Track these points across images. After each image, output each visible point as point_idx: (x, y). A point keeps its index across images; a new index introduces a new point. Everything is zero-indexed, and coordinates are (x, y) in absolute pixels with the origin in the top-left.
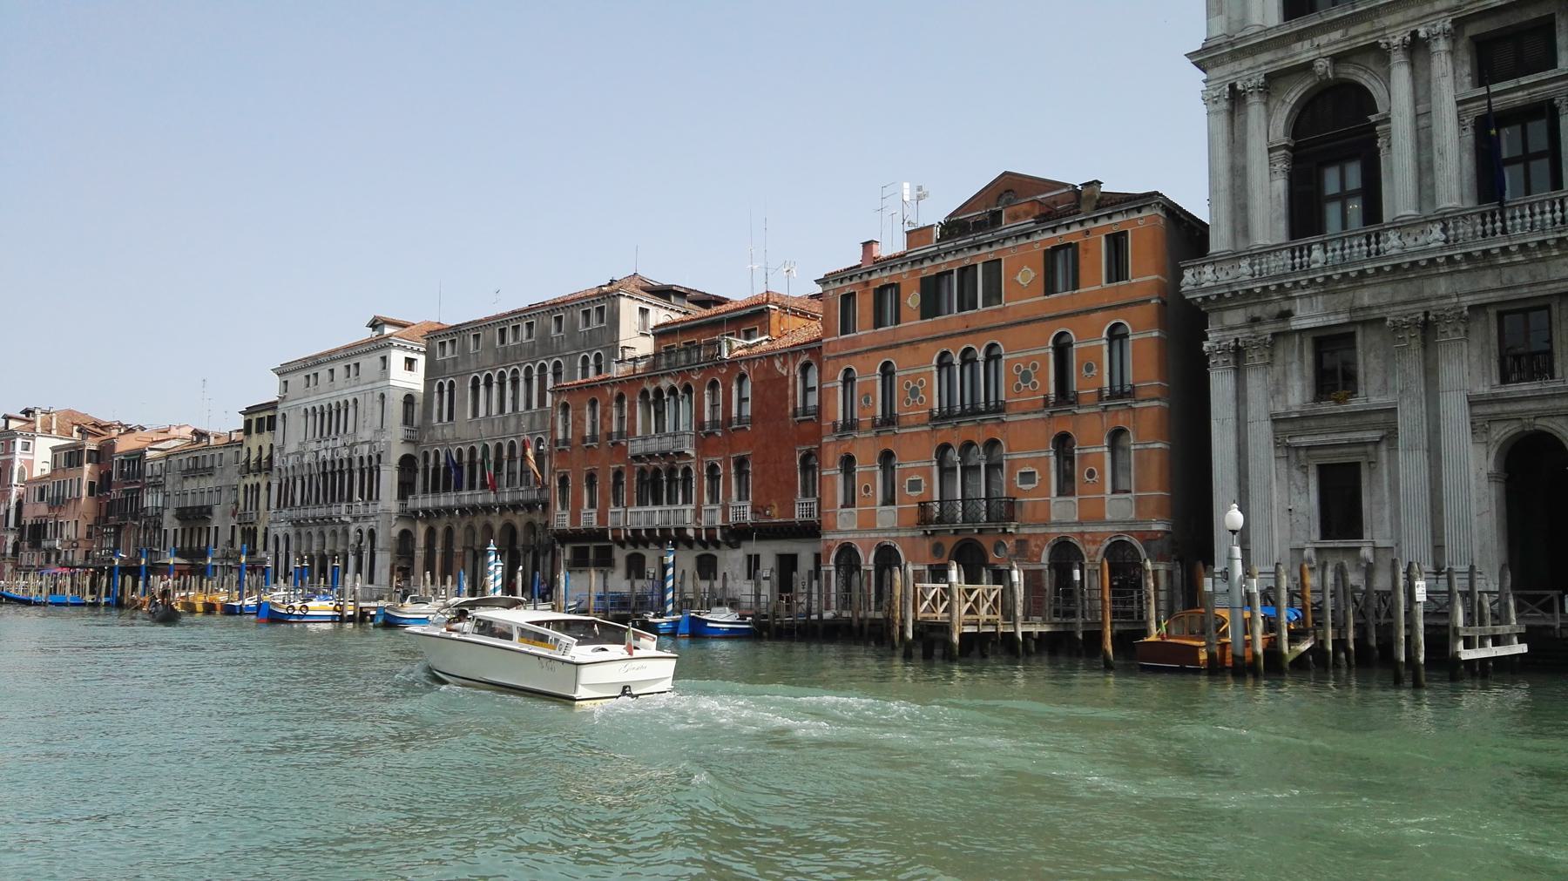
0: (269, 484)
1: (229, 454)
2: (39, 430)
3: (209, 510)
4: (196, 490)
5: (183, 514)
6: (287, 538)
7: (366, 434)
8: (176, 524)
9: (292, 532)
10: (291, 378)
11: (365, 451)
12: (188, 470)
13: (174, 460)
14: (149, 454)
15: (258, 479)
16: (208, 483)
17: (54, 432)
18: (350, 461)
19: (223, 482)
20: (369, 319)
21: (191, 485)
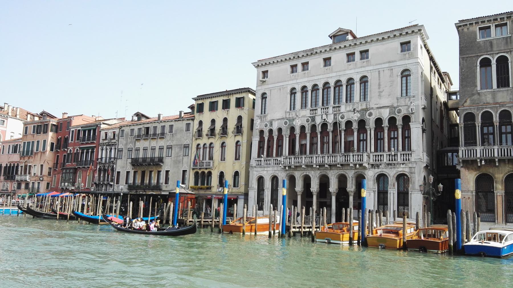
0: (223, 145)
1: (182, 125)
2: (10, 114)
3: (161, 160)
4: (146, 148)
5: (135, 163)
6: (275, 179)
7: (385, 101)
8: (129, 168)
9: (282, 176)
10: (271, 69)
11: (385, 115)
12: (139, 136)
13: (127, 130)
14: (103, 126)
15: (211, 140)
16: (157, 143)
17: (18, 117)
18: (362, 123)
19: (174, 143)
20: (333, 30)
21: (142, 144)
